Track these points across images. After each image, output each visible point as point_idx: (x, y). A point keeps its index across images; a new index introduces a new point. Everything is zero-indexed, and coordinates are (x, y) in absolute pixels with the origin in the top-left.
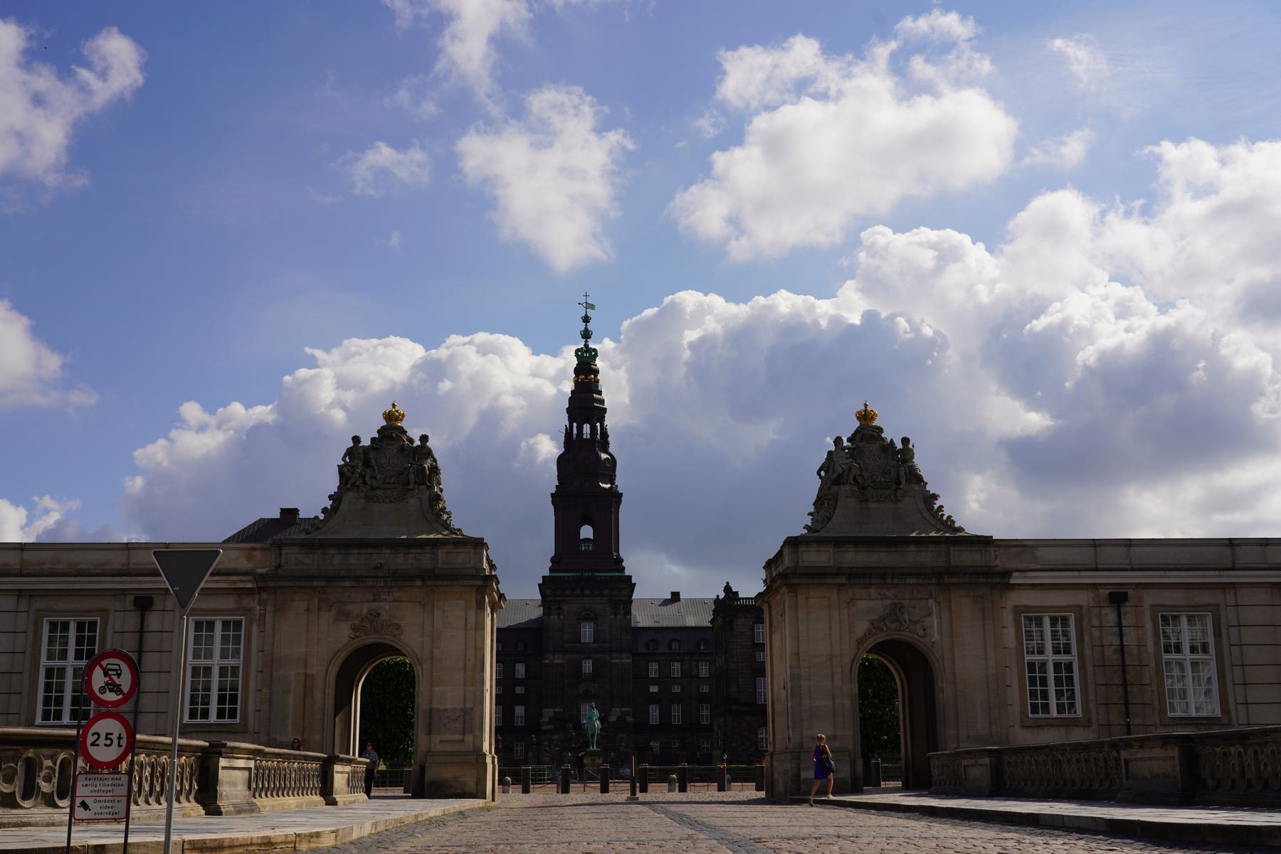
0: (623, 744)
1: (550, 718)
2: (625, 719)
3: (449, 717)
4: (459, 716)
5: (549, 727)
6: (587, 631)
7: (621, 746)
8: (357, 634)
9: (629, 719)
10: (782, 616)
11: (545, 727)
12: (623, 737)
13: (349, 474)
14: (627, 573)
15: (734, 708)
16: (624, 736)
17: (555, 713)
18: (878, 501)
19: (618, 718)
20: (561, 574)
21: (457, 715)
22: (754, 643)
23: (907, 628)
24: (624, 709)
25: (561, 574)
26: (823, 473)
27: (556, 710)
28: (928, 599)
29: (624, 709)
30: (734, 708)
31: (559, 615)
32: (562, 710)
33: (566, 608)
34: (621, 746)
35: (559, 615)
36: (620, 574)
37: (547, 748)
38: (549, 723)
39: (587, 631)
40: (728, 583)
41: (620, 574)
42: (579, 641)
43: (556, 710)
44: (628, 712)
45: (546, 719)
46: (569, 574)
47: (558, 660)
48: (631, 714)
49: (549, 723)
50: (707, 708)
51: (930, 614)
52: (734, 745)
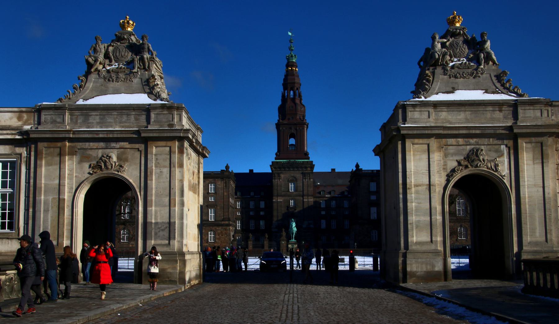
3: (159, 228)
4: (166, 228)
6: (291, 186)
8: (95, 171)
10: (394, 158)
13: (92, 62)
14: (311, 160)
18: (464, 78)
20: (280, 161)
21: (165, 227)
23: (485, 165)
25: (280, 161)
26: (422, 64)
28: (501, 145)
31: (279, 179)
33: (282, 176)
35: (279, 179)
36: (307, 160)
39: (291, 186)
41: (307, 160)
46: (284, 161)
51: (502, 155)
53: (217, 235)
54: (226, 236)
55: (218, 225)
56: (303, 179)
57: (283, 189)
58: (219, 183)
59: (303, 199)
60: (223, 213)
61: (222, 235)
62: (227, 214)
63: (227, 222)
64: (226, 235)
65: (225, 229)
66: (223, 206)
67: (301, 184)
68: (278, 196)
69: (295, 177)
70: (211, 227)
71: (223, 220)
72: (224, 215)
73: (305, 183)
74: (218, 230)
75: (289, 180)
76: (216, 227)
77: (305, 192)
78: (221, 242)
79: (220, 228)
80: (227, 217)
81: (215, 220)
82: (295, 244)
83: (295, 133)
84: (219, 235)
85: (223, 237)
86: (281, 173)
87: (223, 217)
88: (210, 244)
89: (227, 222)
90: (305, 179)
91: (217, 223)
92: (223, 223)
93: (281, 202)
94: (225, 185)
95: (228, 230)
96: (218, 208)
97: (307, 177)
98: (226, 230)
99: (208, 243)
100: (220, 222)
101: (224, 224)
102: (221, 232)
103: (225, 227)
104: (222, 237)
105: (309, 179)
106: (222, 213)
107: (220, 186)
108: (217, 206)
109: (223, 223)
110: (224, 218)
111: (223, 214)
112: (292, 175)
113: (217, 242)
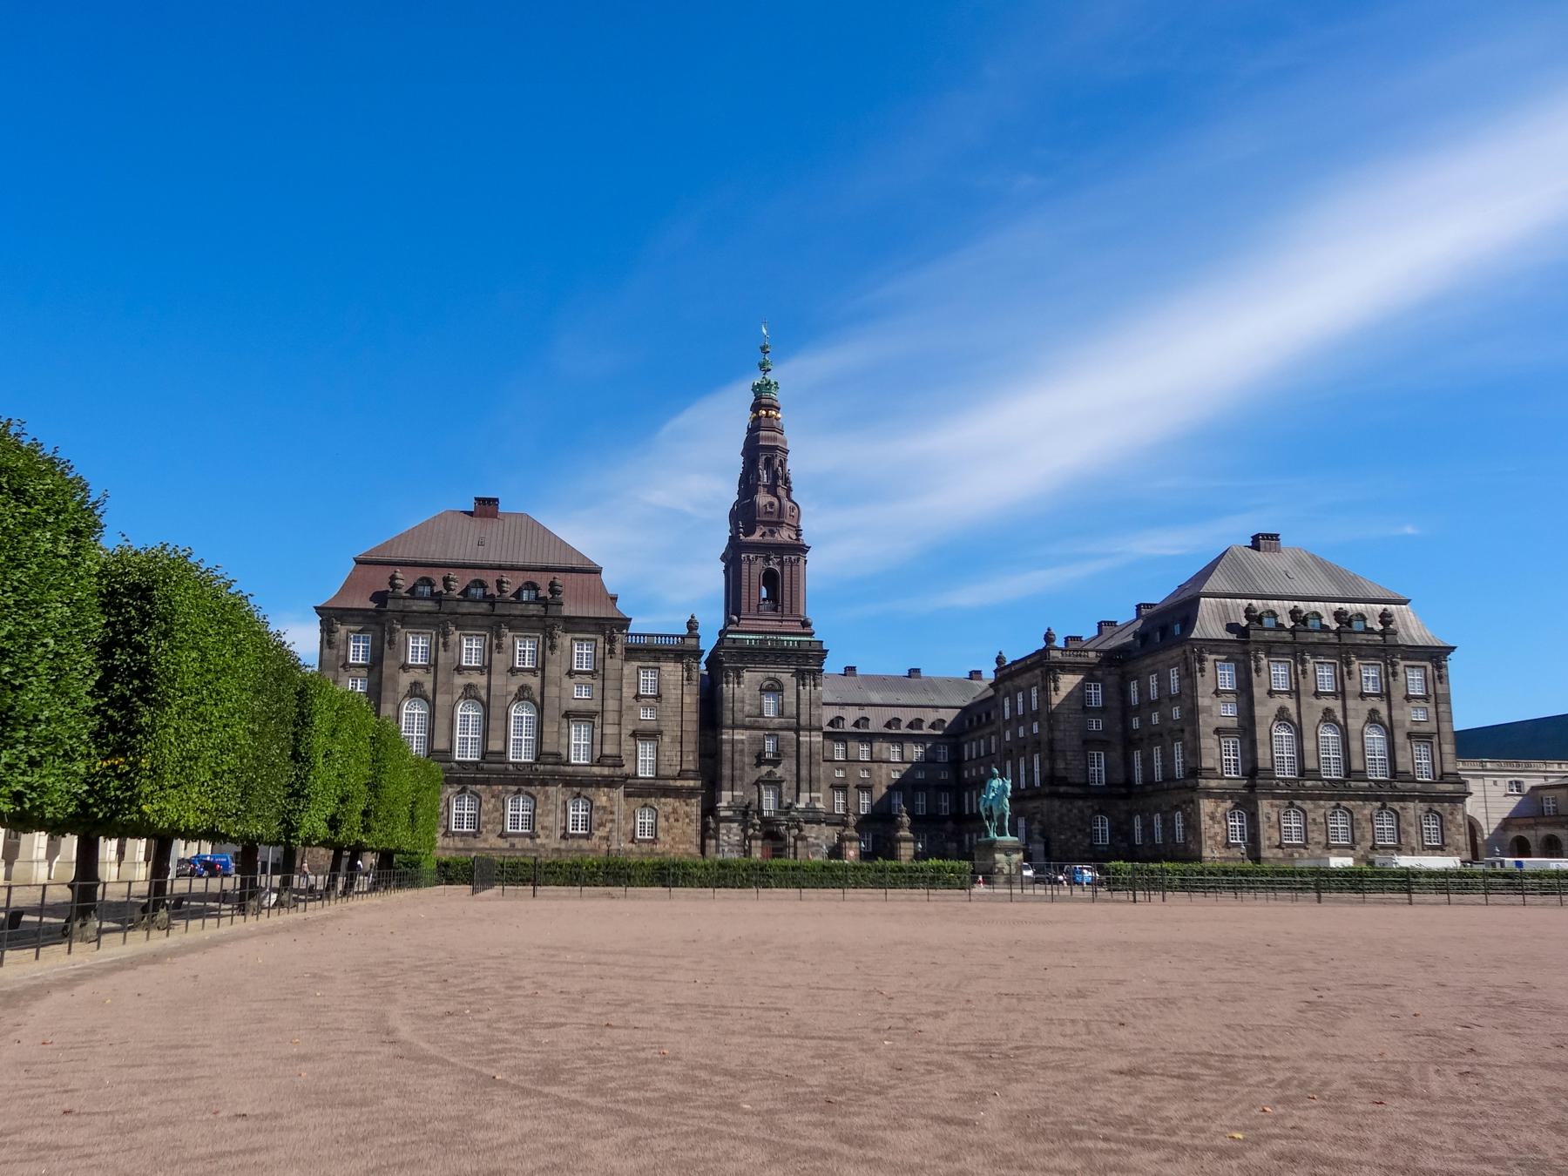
0: (813, 835)
1: (729, 803)
5: (729, 813)
6: (769, 704)
11: (723, 814)
14: (816, 637)
15: (1062, 789)
20: (741, 637)
22: (1084, 707)
25: (741, 637)
30: (1062, 789)
31: (739, 683)
32: (742, 794)
33: (746, 675)
35: (739, 683)
36: (809, 639)
37: (725, 838)
40: (1049, 629)
41: (809, 639)
42: (761, 715)
44: (819, 798)
45: (724, 804)
46: (751, 637)
47: (740, 735)
49: (728, 808)
50: (899, 797)
52: (1063, 837)
54: (688, 824)
55: (667, 792)
56: (798, 685)
57: (747, 708)
58: (670, 669)
59: (798, 736)
61: (677, 820)
62: (691, 758)
63: (691, 783)
64: (687, 820)
66: (679, 734)
67: (794, 700)
68: (734, 727)
69: (777, 681)
71: (681, 775)
73: (802, 696)
75: (764, 687)
77: (804, 720)
78: (673, 839)
81: (657, 777)
82: (1017, 850)
83: (777, 568)
84: (667, 820)
85: (680, 823)
86: (743, 668)
89: (691, 783)
90: (804, 685)
91: (661, 782)
92: (679, 783)
93: (742, 742)
94: (685, 674)
96: (666, 739)
97: (808, 681)
100: (671, 783)
101: (682, 787)
102: (675, 811)
104: (676, 824)
105: (815, 686)
107: (672, 678)
108: (661, 733)
109: (679, 783)
112: (772, 675)
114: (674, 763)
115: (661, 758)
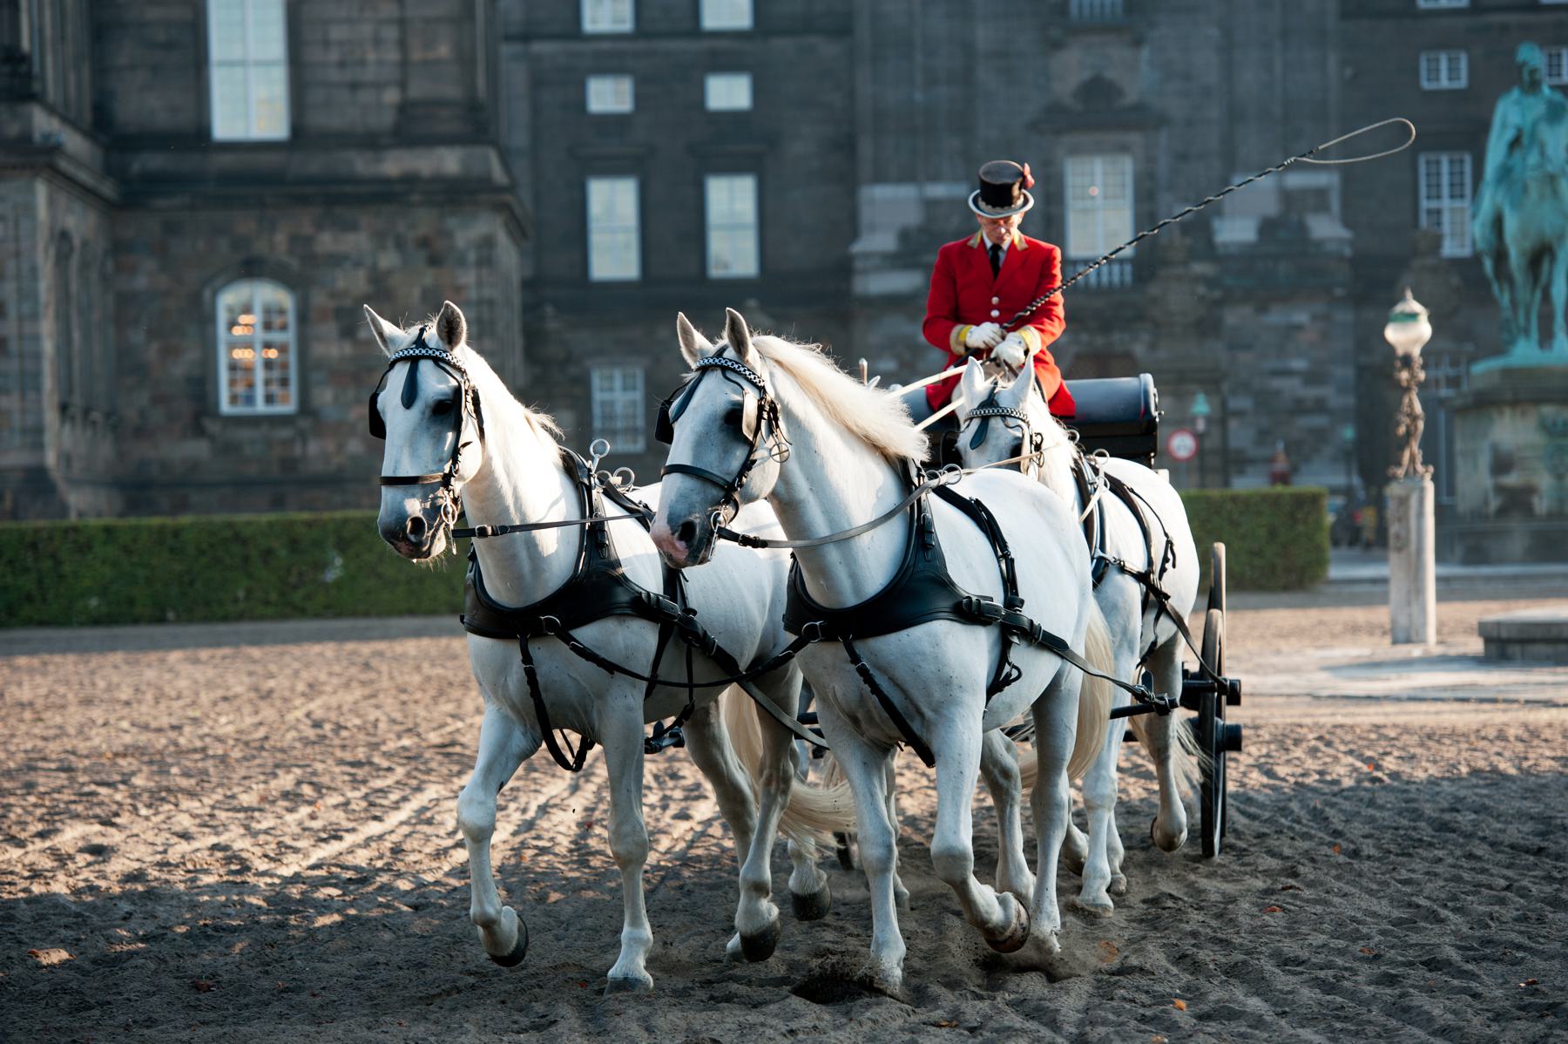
0: (1299, 364)
1: (904, 236)
2: (1302, 228)
7: (1287, 373)
9: (1326, 228)
12: (1299, 328)
16: (1301, 317)
17: (930, 205)
19: (1267, 227)
24: (1295, 180)
27: (938, 191)
29: (1295, 180)
34: (1287, 373)
38: (899, 260)
43: (938, 191)
44: (1321, 194)
45: (877, 240)
48: (1335, 203)
49: (899, 260)
53: (330, 328)
60: (391, 33)
62: (444, 51)
63: (450, 161)
65: (424, 243)
70: (245, 223)
72: (404, 64)
74: (336, 260)
76: (304, 221)
79: (356, 242)
80: (452, 91)
81: (297, 129)
87: (391, 96)
88: (228, 449)
89: (450, 161)
91: (314, 164)
92: (394, 164)
95: (462, 262)
98: (435, 261)
99: (212, 426)
100: (361, 164)
101: (410, 180)
103: (423, 221)
106: (378, 42)
110: (403, 108)
111: (392, 55)
113: (331, 413)
114: (370, 74)
115: (314, 54)
